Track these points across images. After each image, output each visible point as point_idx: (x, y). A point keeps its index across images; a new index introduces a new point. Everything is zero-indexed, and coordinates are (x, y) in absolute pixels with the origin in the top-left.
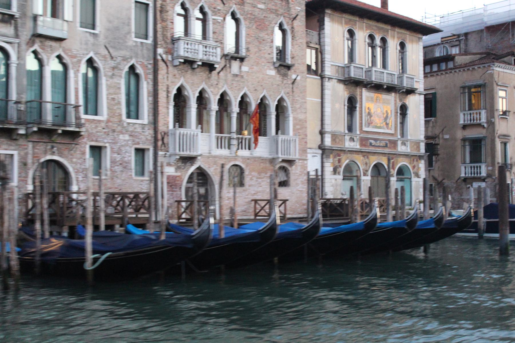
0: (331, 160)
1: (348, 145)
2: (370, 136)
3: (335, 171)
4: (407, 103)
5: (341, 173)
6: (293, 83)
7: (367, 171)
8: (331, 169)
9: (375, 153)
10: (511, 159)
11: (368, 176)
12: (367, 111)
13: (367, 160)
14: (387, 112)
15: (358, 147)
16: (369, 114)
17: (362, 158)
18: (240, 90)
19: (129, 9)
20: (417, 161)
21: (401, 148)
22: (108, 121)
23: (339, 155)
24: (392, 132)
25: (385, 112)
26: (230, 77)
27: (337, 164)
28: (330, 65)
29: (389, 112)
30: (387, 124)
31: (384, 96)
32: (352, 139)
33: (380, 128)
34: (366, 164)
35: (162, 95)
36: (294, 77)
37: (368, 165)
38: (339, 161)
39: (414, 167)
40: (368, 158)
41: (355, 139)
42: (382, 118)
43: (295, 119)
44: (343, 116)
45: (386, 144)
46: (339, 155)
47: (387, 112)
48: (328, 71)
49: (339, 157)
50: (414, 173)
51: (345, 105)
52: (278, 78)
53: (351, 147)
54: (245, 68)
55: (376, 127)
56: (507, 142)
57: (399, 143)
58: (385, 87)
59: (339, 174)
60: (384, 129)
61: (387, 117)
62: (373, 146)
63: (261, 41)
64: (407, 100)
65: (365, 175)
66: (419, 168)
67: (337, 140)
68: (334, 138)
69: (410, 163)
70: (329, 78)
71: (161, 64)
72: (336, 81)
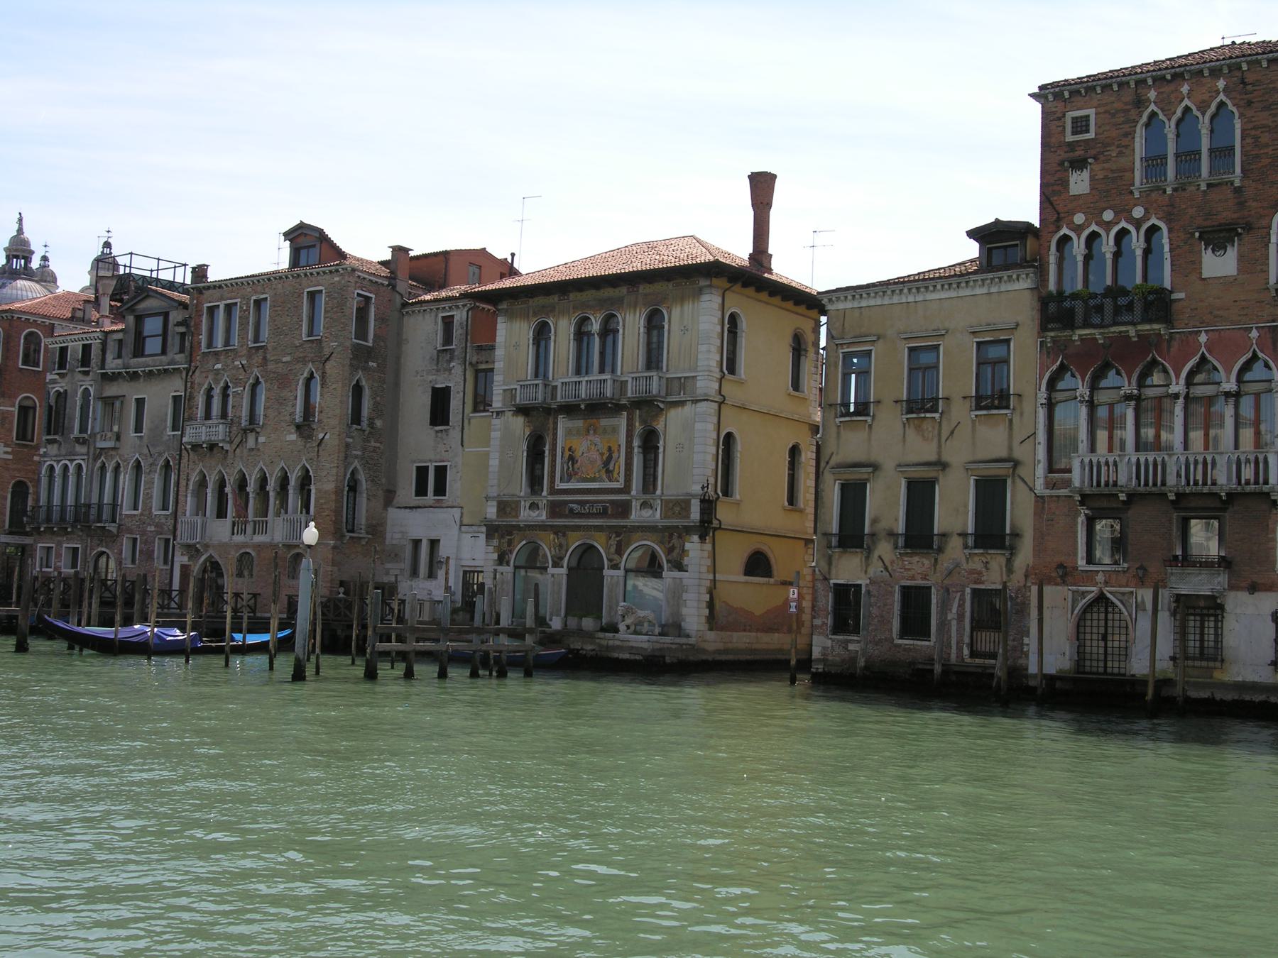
0: (495, 542)
1: (526, 515)
3: (502, 560)
4: (660, 427)
6: (319, 445)
7: (561, 559)
8: (495, 556)
9: (577, 528)
10: (875, 521)
12: (567, 454)
13: (563, 540)
14: (610, 449)
15: (544, 517)
16: (572, 458)
18: (255, 465)
19: (167, 406)
20: (680, 537)
21: (637, 515)
22: (141, 514)
23: (510, 534)
26: (245, 451)
27: (505, 547)
29: (615, 448)
30: (608, 472)
31: (605, 422)
32: (533, 506)
33: (593, 480)
35: (183, 483)
36: (321, 436)
38: (510, 543)
39: (670, 551)
40: (564, 535)
42: (599, 462)
43: (318, 491)
45: (605, 509)
46: (510, 534)
47: (610, 449)
48: (497, 403)
50: (668, 561)
52: (300, 442)
54: (262, 439)
56: (867, 480)
57: (635, 505)
59: (508, 564)
60: (601, 480)
61: (610, 458)
63: (281, 401)
65: (555, 565)
66: (684, 552)
67: (508, 510)
69: (661, 543)
70: (498, 413)
71: (184, 453)
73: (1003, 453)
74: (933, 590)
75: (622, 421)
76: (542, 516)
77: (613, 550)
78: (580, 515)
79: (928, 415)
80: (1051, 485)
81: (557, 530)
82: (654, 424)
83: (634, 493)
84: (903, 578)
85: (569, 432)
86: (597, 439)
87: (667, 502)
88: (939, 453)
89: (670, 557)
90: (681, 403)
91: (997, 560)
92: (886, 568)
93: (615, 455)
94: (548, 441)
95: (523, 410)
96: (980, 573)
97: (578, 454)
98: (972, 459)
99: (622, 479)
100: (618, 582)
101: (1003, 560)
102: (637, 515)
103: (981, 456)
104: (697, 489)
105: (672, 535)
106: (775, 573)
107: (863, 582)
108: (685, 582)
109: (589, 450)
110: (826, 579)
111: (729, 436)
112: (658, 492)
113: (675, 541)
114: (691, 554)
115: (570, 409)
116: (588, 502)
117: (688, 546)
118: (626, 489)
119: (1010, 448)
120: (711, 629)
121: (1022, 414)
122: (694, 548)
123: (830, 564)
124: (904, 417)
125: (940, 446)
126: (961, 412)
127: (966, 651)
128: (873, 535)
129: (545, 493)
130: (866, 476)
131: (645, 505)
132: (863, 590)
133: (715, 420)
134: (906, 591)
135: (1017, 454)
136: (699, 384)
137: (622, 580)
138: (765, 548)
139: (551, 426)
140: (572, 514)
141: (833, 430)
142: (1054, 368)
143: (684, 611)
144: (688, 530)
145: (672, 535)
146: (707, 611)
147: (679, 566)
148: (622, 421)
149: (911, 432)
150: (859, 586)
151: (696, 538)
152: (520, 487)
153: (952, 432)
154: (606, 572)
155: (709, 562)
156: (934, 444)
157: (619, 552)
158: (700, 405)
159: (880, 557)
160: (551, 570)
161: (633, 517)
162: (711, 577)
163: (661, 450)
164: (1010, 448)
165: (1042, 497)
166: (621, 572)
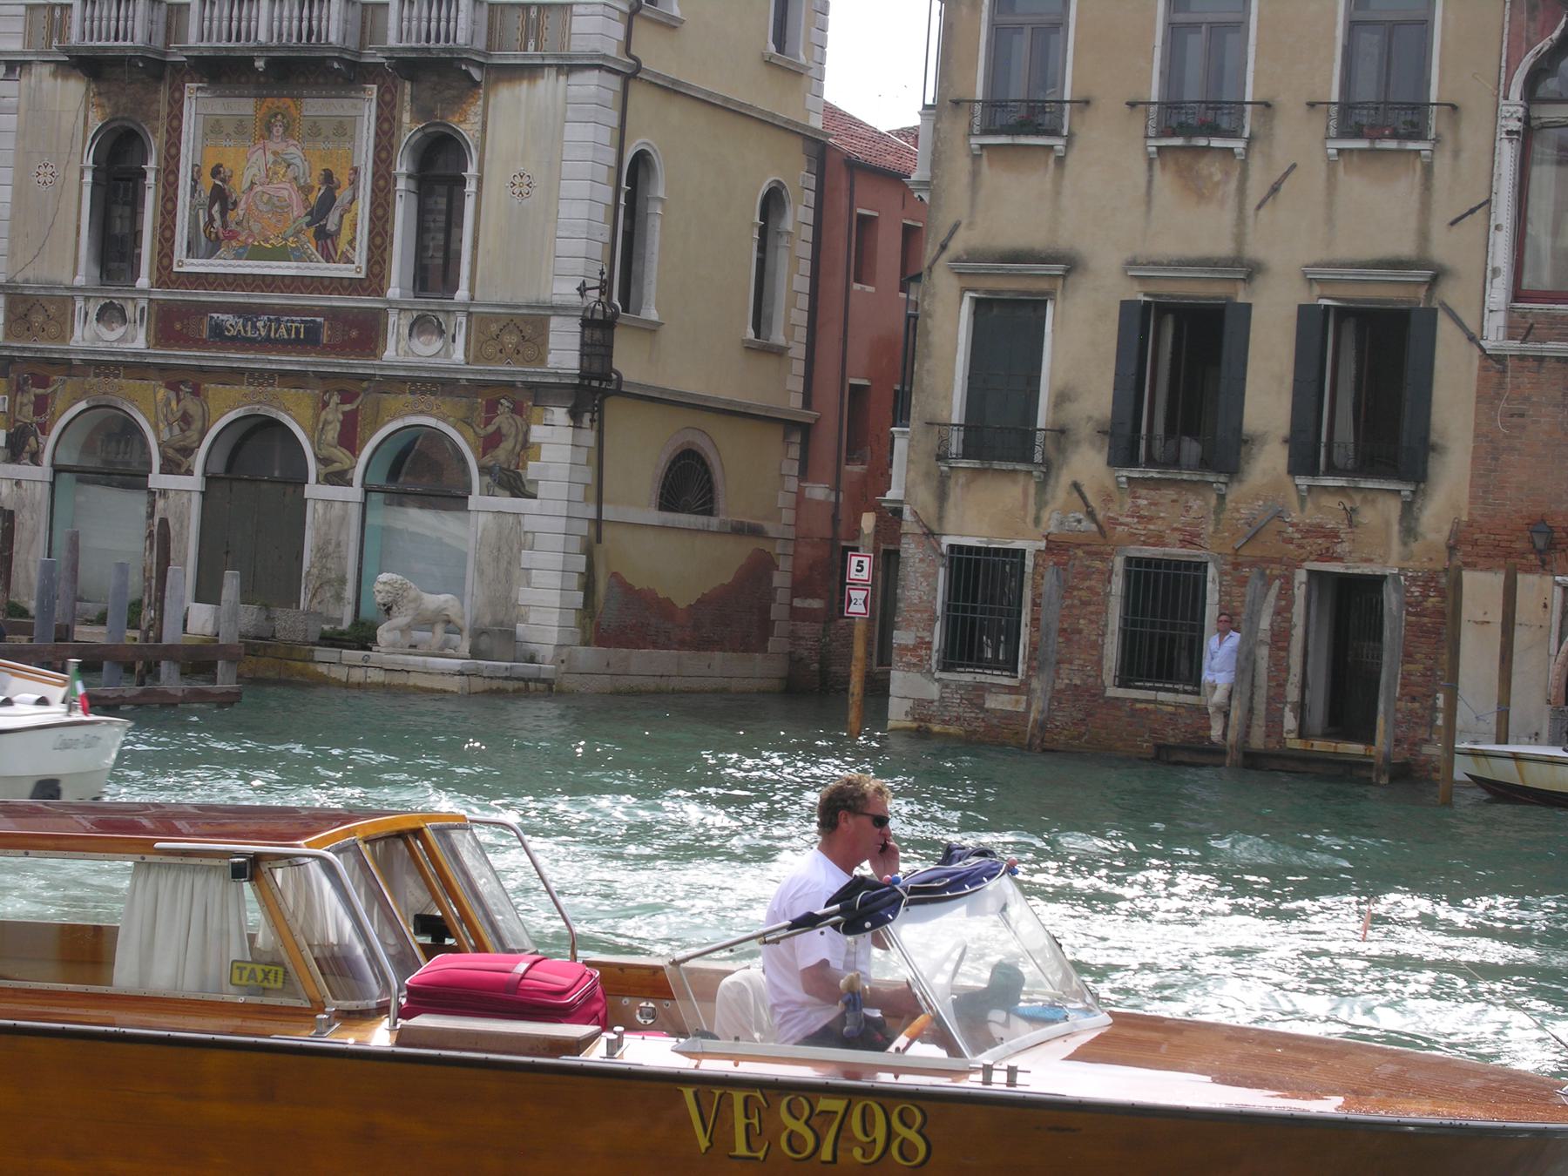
1: (87, 335)
2: (203, 296)
4: (468, 129)
5: (46, 458)
7: (188, 452)
9: (233, 375)
10: (1062, 398)
11: (189, 472)
12: (207, 183)
13: (192, 406)
14: (328, 177)
16: (221, 196)
17: (162, 393)
20: (517, 409)
21: (400, 349)
23: (43, 382)
24: (355, 268)
25: (315, 180)
27: (27, 415)
28: (22, 10)
29: (342, 176)
31: (315, 107)
32: (110, 313)
34: (186, 419)
37: (197, 425)
38: (41, 405)
39: (490, 443)
40: (196, 392)
41: (129, 312)
42: (297, 210)
44: (74, 216)
45: (313, 333)
46: (43, 382)
47: (328, 177)
49: (40, 391)
50: (483, 470)
51: (82, 172)
53: (101, 346)
55: (259, 254)
56: (1050, 294)
57: (397, 325)
58: (260, 64)
60: (301, 256)
61: (327, 202)
62: (233, 338)
64: (475, 110)
65: (169, 467)
66: (526, 448)
67: (38, 319)
68: (21, 309)
69: (464, 422)
72: (46, 70)
73: (1405, 247)
74: (1212, 571)
75: (365, 110)
76: (136, 340)
77: (332, 434)
78: (241, 342)
79: (1216, 143)
80: (1519, 328)
81: (175, 378)
82: (453, 121)
83: (393, 292)
84: (1133, 537)
85: (213, 128)
86: (293, 151)
87: (486, 319)
88: (1239, 238)
89: (488, 460)
90: (530, 71)
91: (1380, 508)
92: (1091, 514)
93: (343, 195)
94: (156, 145)
95: (89, 66)
96: (1333, 535)
97: (238, 187)
98: (1320, 255)
99: (361, 255)
100: (343, 519)
101: (1393, 508)
102: (400, 349)
103: (1343, 251)
104: (565, 291)
105: (500, 401)
106: (721, 503)
107: (1031, 545)
108: (529, 523)
109: (269, 179)
110: (931, 534)
111: (642, 159)
112: (462, 294)
113: (503, 420)
114: (546, 454)
115: (221, 70)
116: (262, 309)
117: (537, 433)
118: (374, 281)
119: (1424, 236)
120: (585, 643)
121: (1456, 154)
122: (554, 441)
123: (942, 496)
124: (1154, 143)
125: (1241, 220)
126: (1300, 141)
127: (1290, 722)
128: (1060, 433)
129: (143, 282)
130: (1043, 285)
131: (422, 325)
132: (1029, 562)
133: (613, 118)
134: (1143, 574)
135: (1443, 247)
136: (578, 25)
137: (355, 513)
138: (702, 443)
139: (164, 110)
140: (220, 337)
141: (963, 164)
142: (1545, 44)
143: (525, 595)
144: (542, 393)
145: (500, 401)
146: (579, 597)
147: (513, 483)
148: (365, 110)
149: (1165, 181)
150: (1021, 553)
151: (560, 415)
152: (71, 262)
153: (1275, 189)
154: (313, 490)
155: (587, 475)
156: (1228, 217)
157: (350, 439)
158: (577, 78)
159: (1076, 486)
160: (157, 480)
161: (389, 354)
162: (592, 514)
163: (471, 187)
164: (1424, 236)
165: (1499, 359)
166: (354, 493)
